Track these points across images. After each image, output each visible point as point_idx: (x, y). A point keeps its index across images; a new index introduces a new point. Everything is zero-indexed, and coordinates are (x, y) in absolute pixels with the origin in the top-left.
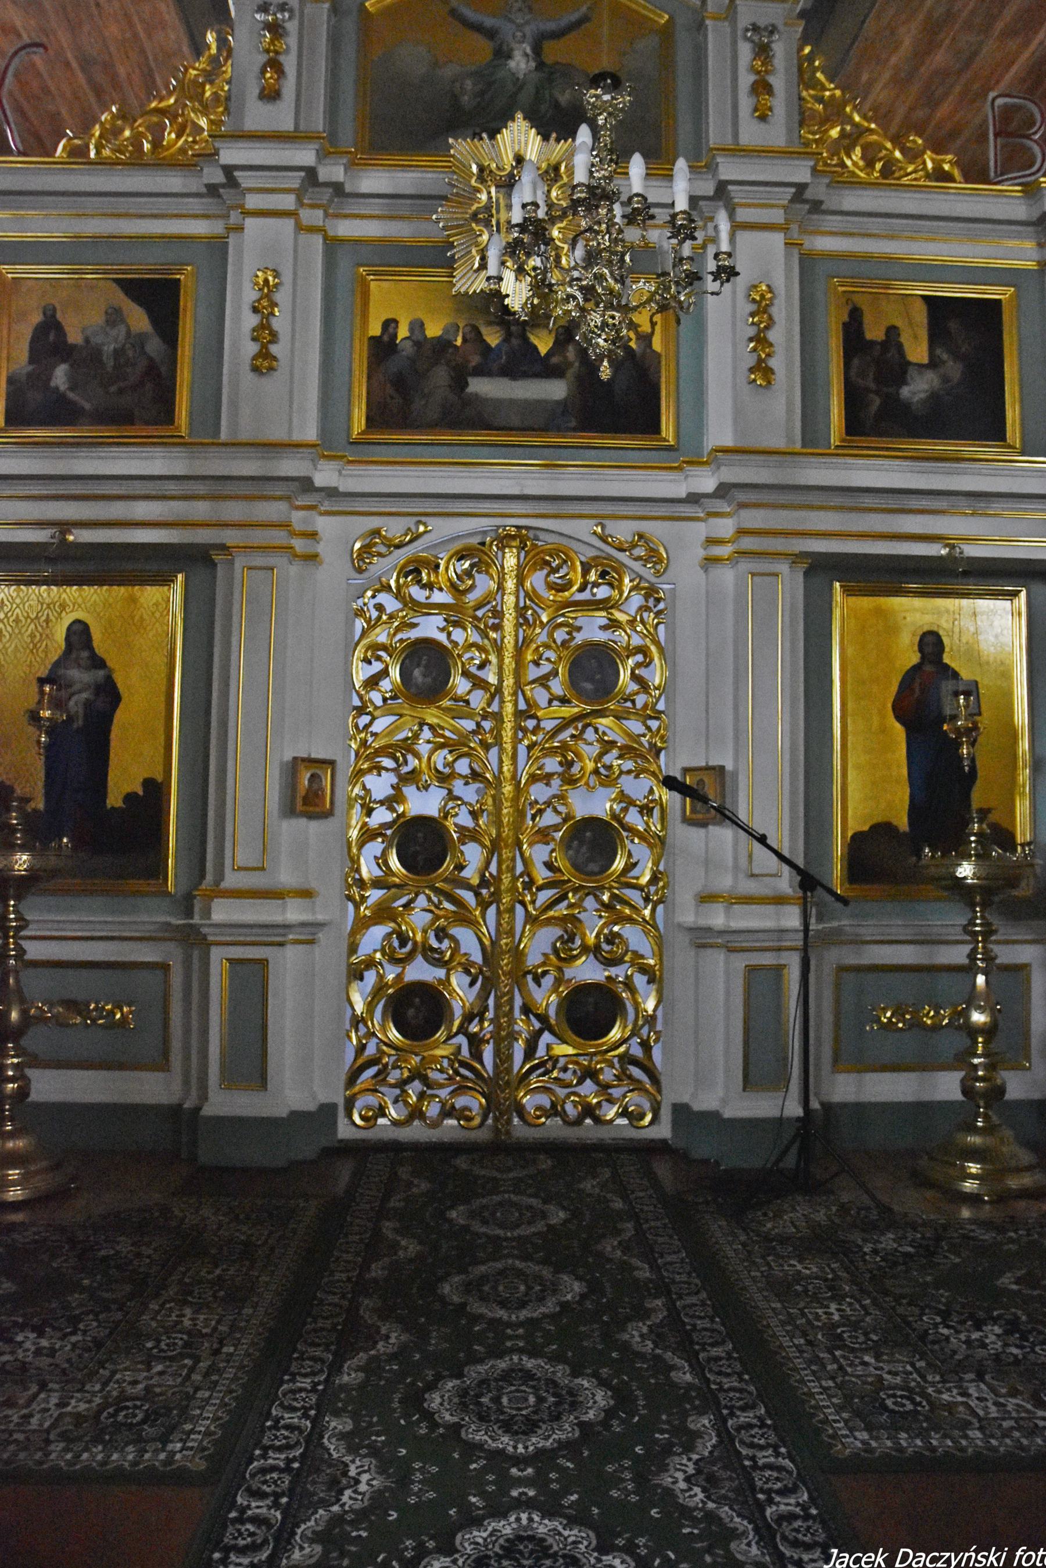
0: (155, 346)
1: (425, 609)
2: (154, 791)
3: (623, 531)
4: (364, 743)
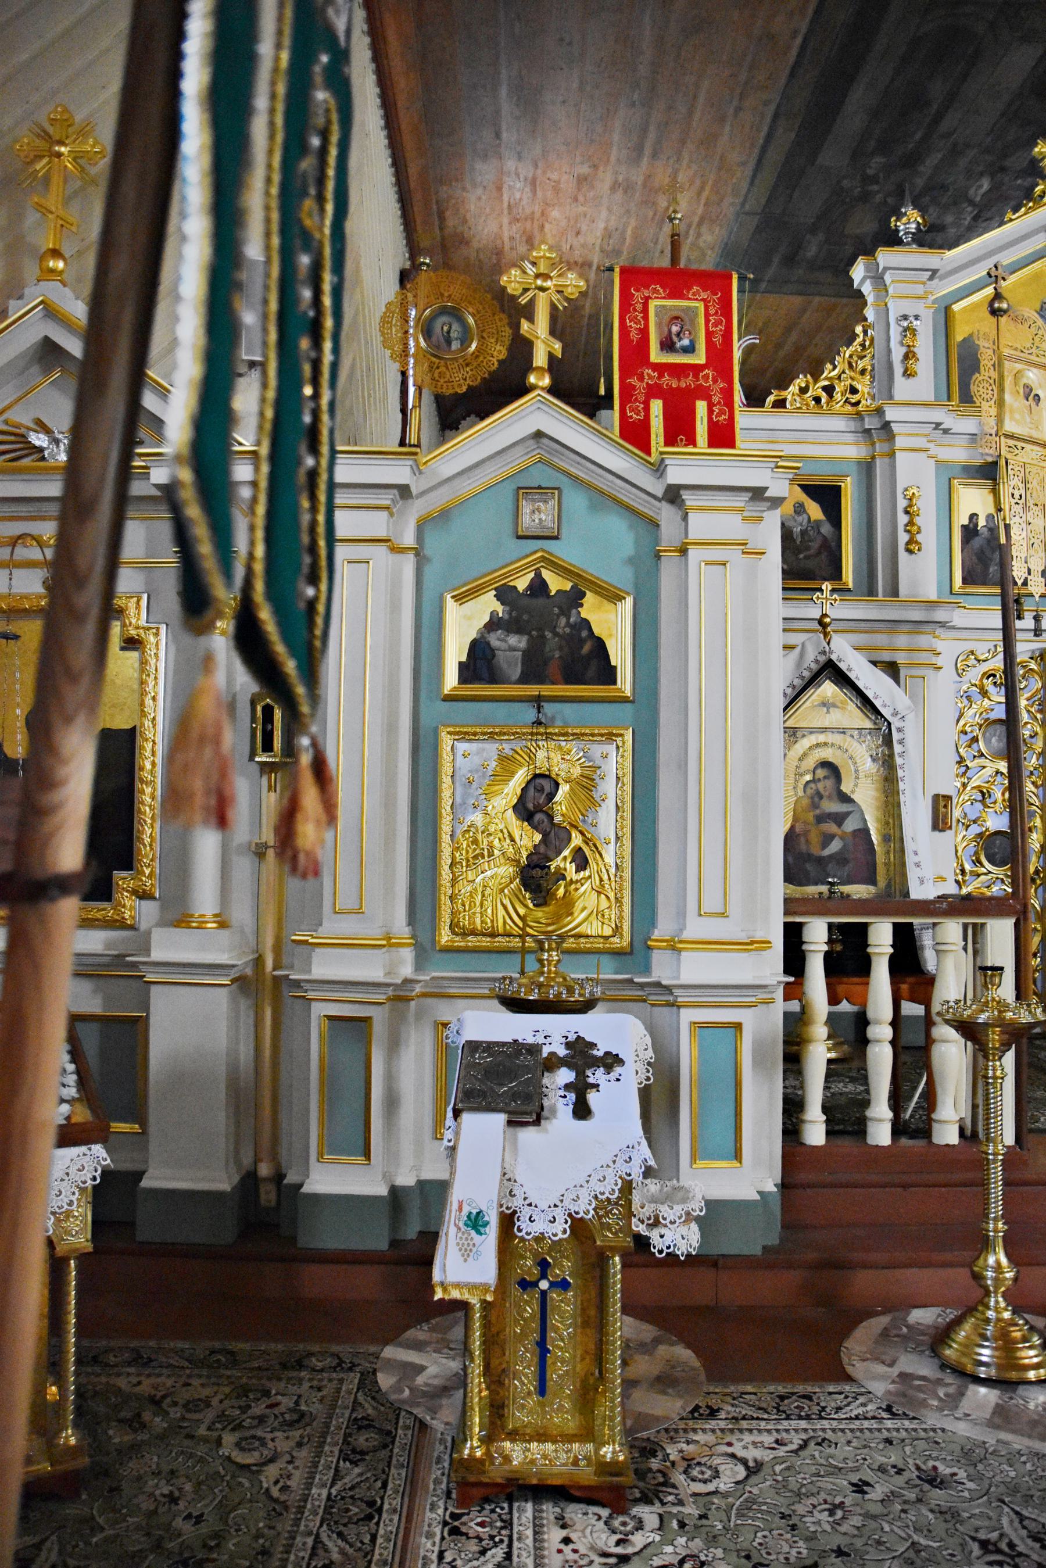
0: (826, 529)
4: (964, 785)
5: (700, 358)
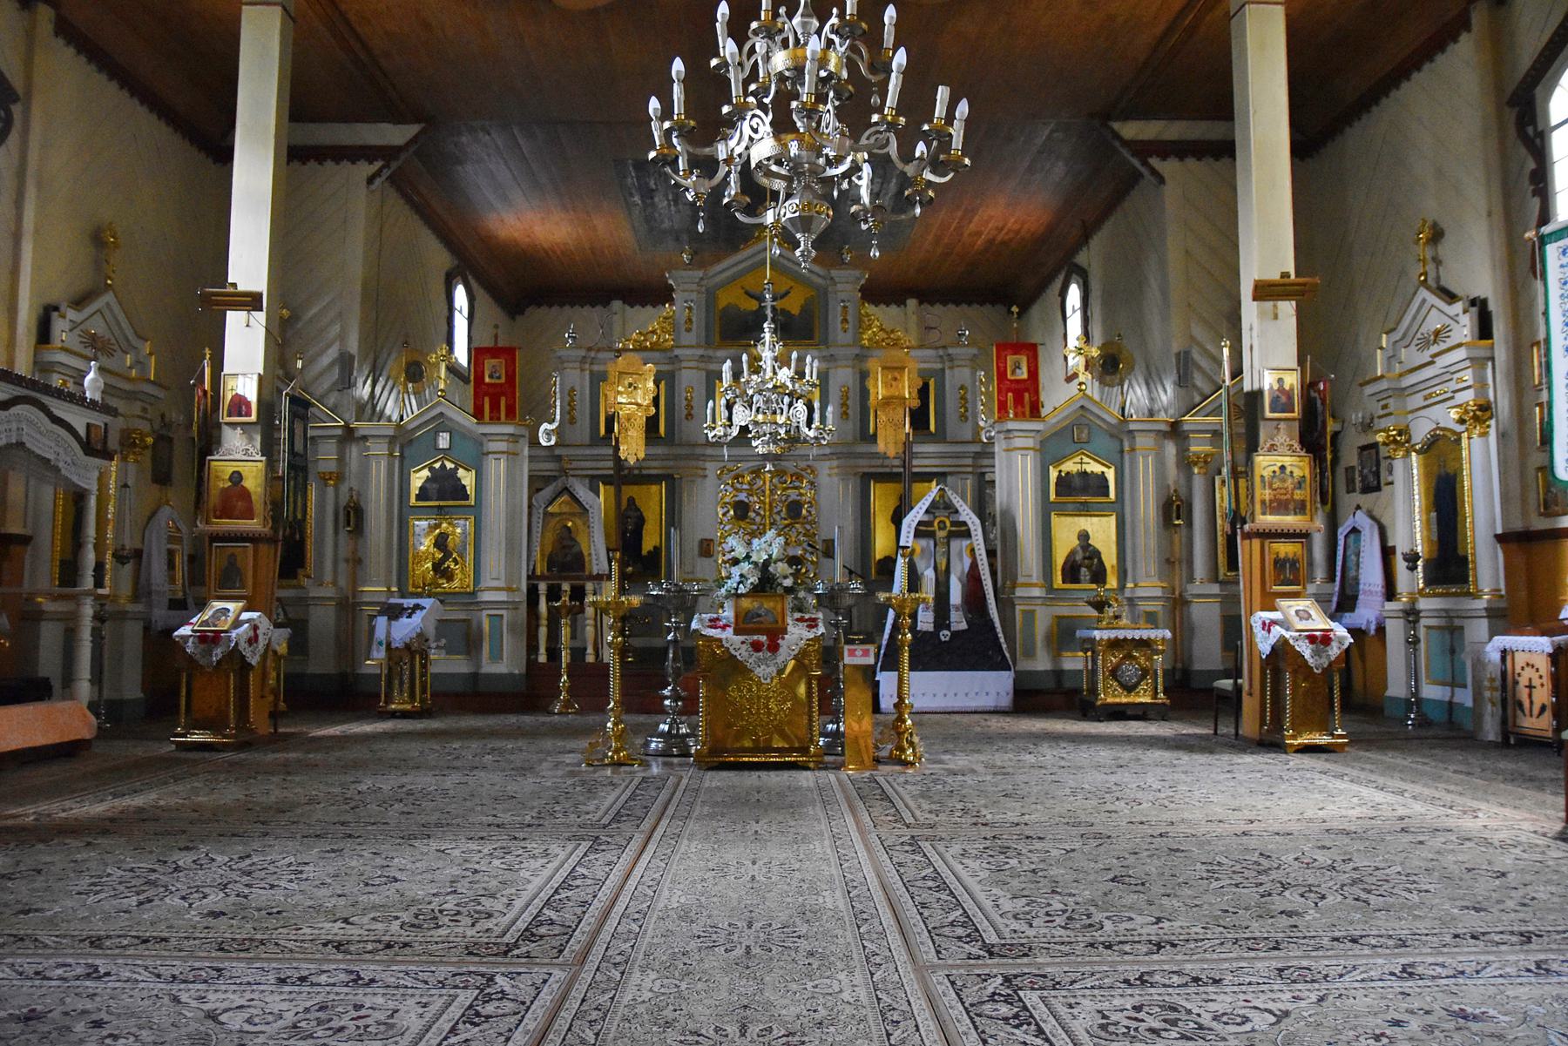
1: (741, 491)
2: (657, 549)
3: (803, 464)
5: (503, 380)
